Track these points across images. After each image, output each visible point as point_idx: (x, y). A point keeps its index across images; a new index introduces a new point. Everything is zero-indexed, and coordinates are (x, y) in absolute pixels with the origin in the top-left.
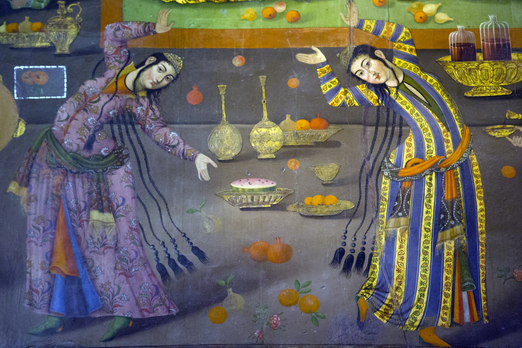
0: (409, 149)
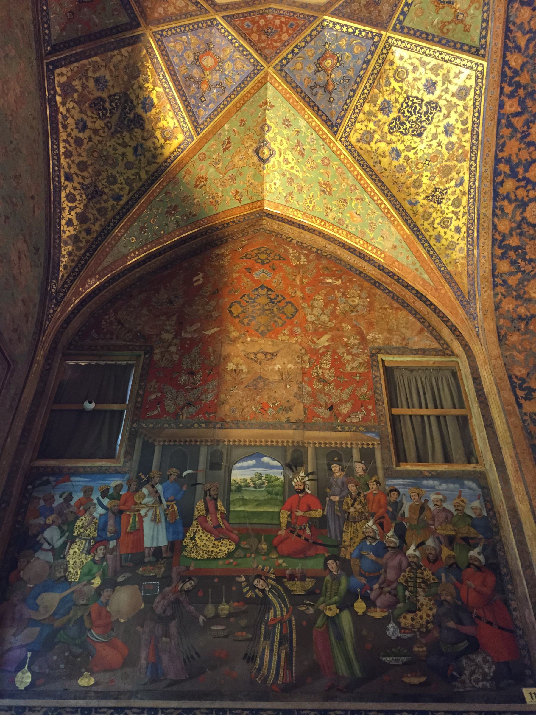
0: (272, 615)
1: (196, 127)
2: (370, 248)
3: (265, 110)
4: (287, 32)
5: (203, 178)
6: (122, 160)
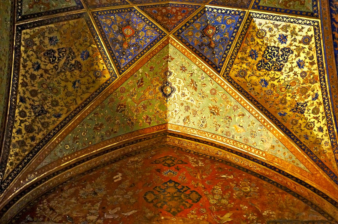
1: (119, 70)
2: (253, 151)
3: (168, 61)
4: (181, 15)
5: (122, 105)
6: (64, 90)
